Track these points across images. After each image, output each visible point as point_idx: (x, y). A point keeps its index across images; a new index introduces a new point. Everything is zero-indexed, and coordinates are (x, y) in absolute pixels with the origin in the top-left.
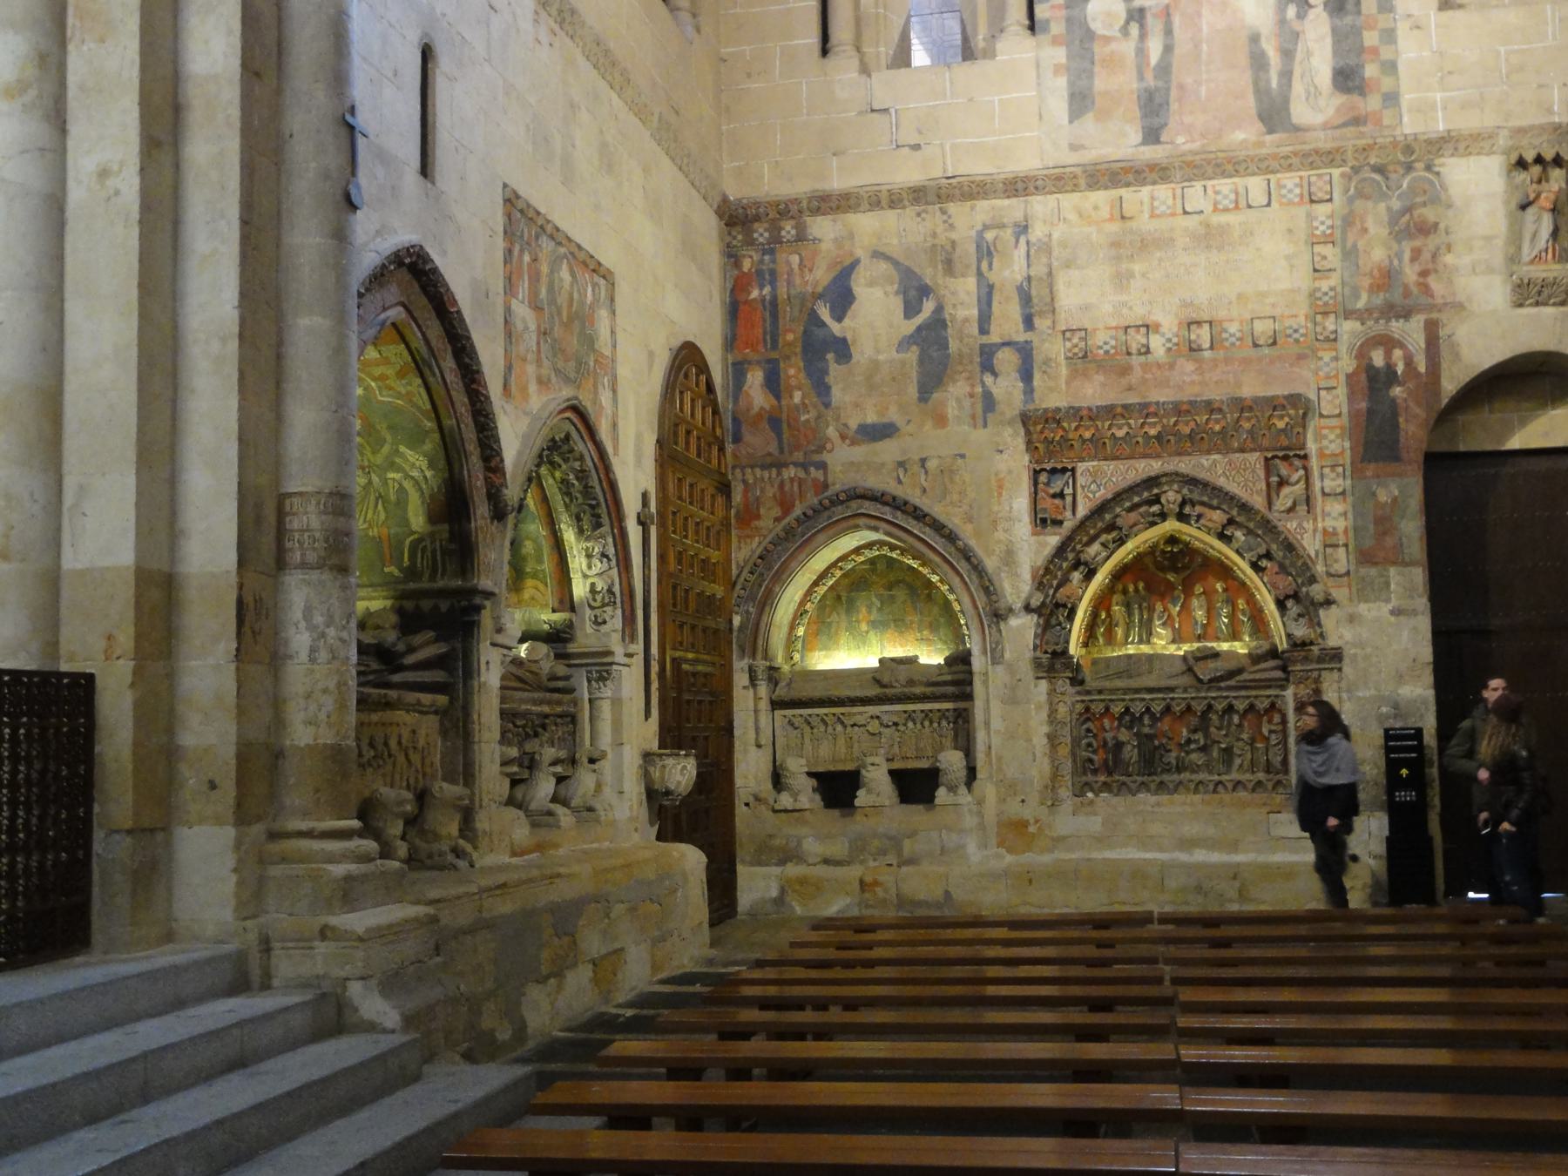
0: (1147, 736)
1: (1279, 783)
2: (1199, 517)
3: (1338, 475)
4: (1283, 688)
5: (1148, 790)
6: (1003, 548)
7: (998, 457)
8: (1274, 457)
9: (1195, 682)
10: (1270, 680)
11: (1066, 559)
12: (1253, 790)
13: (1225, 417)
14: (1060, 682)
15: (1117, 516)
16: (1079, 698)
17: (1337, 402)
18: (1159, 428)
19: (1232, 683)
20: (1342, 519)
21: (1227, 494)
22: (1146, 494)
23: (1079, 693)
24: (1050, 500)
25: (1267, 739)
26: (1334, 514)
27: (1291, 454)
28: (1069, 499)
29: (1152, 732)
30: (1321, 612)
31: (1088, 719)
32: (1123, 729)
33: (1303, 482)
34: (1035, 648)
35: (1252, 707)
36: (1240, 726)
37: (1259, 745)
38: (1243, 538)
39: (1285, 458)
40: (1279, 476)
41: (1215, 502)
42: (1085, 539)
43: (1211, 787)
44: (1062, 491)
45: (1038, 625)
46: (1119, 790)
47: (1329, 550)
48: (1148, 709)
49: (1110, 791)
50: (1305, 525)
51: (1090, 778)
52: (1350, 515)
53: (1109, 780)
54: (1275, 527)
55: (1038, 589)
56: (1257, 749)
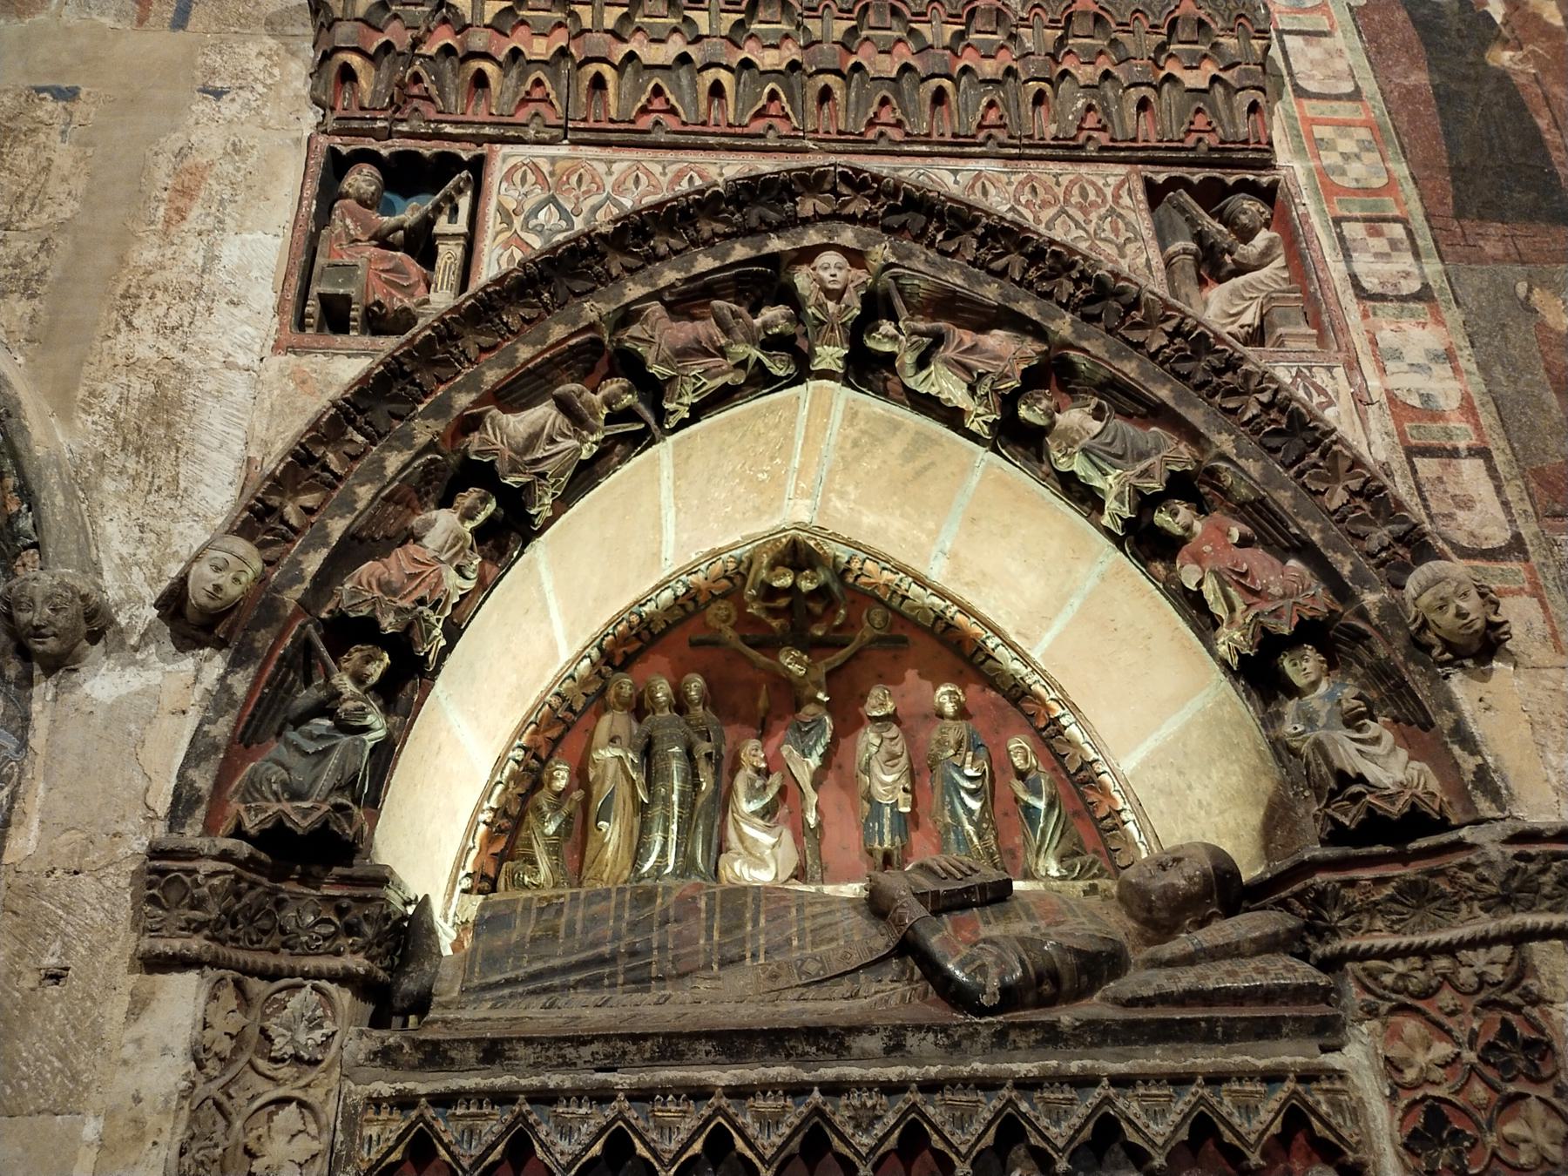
2: (938, 339)
3: (1394, 244)
4: (1329, 1032)
6: (140, 387)
7: (204, 107)
8: (1173, 183)
9: (938, 1012)
10: (1266, 995)
11: (406, 440)
13: (1013, 37)
14: (302, 1000)
15: (627, 316)
16: (385, 1089)
17: (1340, 65)
18: (791, 52)
19: (1095, 1007)
20: (1443, 370)
21: (1037, 256)
22: (740, 252)
23: (386, 1057)
24: (372, 251)
26: (1415, 355)
27: (1231, 180)
28: (448, 254)
30: (1460, 686)
33: (1280, 261)
34: (183, 803)
35: (1203, 1127)
38: (1097, 426)
39: (1212, 195)
40: (1199, 237)
41: (991, 292)
42: (492, 377)
44: (428, 222)
45: (220, 699)
47: (1427, 467)
50: (1321, 377)
52: (1466, 361)
54: (1232, 364)
55: (244, 529)
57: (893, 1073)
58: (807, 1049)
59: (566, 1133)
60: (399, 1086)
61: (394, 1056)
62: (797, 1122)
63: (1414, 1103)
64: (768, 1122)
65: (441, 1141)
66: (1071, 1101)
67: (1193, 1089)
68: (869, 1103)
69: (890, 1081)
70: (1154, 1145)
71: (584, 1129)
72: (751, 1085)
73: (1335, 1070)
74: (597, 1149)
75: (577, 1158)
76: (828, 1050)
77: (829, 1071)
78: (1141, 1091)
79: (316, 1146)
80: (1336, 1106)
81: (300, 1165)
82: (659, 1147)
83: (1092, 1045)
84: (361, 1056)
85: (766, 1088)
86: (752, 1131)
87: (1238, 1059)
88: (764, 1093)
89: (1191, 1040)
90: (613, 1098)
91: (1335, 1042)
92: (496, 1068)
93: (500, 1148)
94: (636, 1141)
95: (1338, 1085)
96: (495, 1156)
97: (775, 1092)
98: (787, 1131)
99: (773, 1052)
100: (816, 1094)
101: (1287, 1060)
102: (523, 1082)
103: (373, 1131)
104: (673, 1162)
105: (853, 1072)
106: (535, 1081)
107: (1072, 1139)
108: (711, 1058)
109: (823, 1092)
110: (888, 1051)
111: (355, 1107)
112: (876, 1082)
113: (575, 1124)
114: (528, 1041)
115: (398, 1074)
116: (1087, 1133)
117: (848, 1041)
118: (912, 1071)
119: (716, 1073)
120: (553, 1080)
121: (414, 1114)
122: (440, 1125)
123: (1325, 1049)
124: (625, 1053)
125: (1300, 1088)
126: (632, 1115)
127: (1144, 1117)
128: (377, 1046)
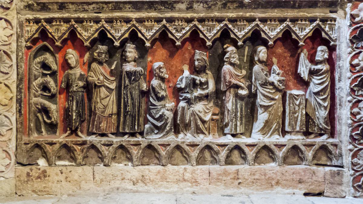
0: (129, 74)
1: (324, 148)
5: (130, 159)
12: (285, 160)
16: (31, 17)
25: (305, 84)
29: (139, 69)
31: (45, 49)
32: (94, 65)
36: (267, 64)
37: (295, 92)
43: (223, 154)
46: (86, 157)
48: (134, 37)
49: (73, 159)
51: (45, 137)
53: (73, 138)
56: (293, 97)
57: (189, 15)
58: (161, 7)
59: (86, 30)
60: (35, 16)
61: (32, 7)
62: (157, 29)
63: (357, 28)
64: (149, 29)
65: (49, 32)
66: (245, 25)
67: (285, 22)
68: (181, 24)
69: (188, 18)
70: (270, 38)
71: (92, 29)
72: (143, 18)
73: (333, 18)
74: (96, 35)
75: (90, 37)
76: (168, 8)
77: (168, 14)
78: (269, 23)
79: (12, 32)
80: (331, 29)
81: (8, 37)
82: (114, 35)
83: (255, 8)
84: (22, 7)
85: (149, 19)
86: (144, 31)
87: (302, 14)
88: (148, 21)
89: (287, 8)
90: (101, 21)
91: (335, 9)
92: (64, 11)
93: (67, 34)
94: (108, 34)
95: (333, 23)
96: (66, 36)
97: (151, 20)
98: (154, 31)
99: (150, 8)
100: (164, 20)
101: (318, 14)
102: (72, 16)
103: (29, 29)
104: (119, 39)
105: (176, 15)
106: (76, 16)
107: (244, 36)
108: (130, 10)
109: (166, 21)
110: (187, 9)
111: (22, 22)
112: (183, 18)
113: (89, 28)
114: (73, 3)
115: (34, 13)
116: (249, 34)
117: (175, 5)
118: (195, 15)
119: (132, 14)
120: (82, 15)
121: (40, 24)
122: (48, 27)
123: (331, 12)
124: (103, 8)
125: (320, 23)
126: (106, 25)
127: (268, 31)
128: (26, 4)
